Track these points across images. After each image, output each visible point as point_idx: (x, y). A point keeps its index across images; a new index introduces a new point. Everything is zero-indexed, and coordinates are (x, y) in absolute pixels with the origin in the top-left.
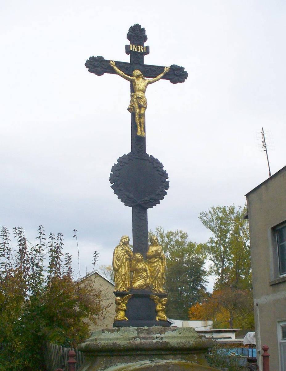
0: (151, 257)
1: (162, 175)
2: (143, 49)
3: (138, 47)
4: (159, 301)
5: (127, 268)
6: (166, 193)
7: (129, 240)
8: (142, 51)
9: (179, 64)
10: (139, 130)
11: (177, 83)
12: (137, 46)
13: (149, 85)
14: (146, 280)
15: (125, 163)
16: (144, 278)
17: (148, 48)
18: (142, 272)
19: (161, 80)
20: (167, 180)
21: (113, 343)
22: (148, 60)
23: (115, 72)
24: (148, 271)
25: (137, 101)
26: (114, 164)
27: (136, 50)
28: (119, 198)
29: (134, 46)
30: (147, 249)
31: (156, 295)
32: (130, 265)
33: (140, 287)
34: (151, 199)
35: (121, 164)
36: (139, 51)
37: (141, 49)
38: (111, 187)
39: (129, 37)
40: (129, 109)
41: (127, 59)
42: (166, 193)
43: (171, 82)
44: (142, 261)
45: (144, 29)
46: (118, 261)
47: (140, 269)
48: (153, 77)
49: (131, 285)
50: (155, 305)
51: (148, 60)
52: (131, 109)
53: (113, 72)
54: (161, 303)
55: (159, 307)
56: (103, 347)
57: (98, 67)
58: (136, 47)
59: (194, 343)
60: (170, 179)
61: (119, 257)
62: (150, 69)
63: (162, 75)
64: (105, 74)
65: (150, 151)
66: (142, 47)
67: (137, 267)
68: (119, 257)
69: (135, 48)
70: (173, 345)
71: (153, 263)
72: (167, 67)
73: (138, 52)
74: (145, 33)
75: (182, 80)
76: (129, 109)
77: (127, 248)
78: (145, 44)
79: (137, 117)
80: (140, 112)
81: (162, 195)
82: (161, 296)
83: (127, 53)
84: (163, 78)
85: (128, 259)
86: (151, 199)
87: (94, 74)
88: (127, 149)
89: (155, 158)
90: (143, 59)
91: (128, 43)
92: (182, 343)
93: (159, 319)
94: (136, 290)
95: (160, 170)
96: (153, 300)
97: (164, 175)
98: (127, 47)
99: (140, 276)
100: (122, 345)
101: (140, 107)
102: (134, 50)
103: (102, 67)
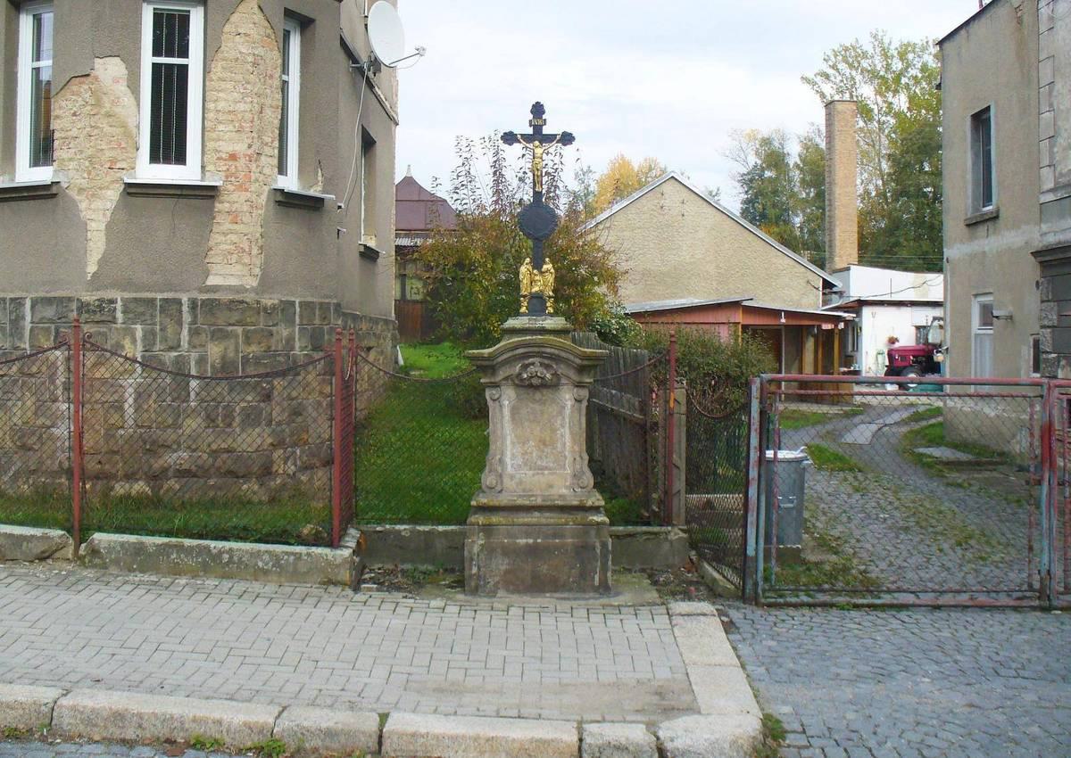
17: (545, 120)
22: (546, 130)
30: (542, 267)
41: (530, 131)
51: (546, 130)
55: (548, 304)
78: (544, 117)
82: (550, 297)
90: (541, 130)
96: (545, 300)
98: (530, 121)
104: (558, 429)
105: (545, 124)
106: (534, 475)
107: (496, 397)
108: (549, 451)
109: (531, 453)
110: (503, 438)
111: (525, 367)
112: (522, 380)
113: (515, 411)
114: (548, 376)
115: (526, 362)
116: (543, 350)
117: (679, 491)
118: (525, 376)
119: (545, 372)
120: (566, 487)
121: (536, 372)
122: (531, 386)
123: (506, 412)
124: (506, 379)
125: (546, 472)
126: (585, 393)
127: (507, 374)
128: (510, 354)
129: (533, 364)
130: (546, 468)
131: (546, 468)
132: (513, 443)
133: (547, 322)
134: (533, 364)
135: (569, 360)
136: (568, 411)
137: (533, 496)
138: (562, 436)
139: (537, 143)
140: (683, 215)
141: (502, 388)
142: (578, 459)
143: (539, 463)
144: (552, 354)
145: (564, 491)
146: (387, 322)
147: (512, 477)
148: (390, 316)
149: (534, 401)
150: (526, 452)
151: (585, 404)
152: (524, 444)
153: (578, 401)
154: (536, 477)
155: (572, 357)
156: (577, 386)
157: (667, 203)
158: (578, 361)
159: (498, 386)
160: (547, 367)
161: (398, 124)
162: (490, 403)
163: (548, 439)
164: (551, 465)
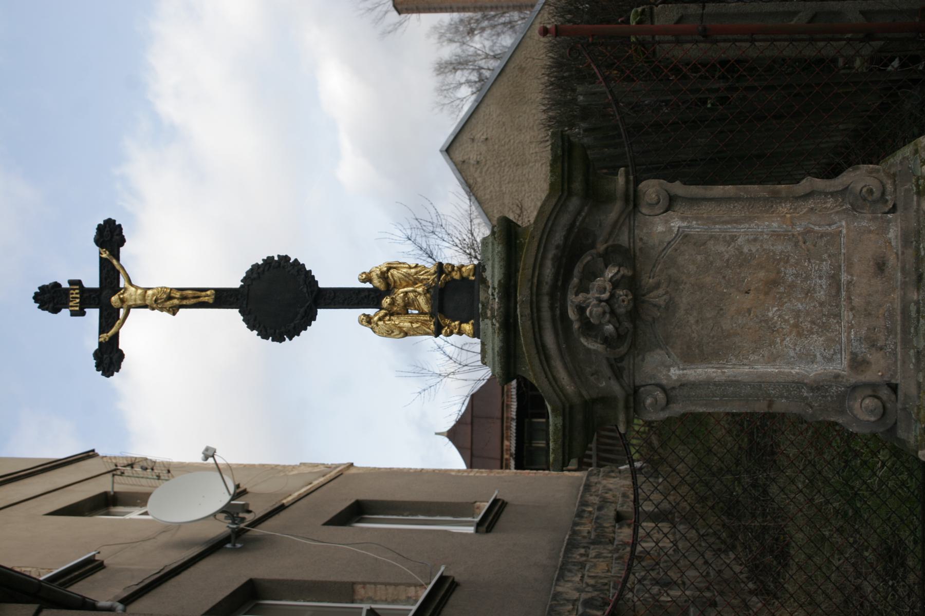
0: (388, 285)
1: (270, 266)
2: (74, 289)
3: (73, 298)
4: (447, 275)
5: (402, 318)
6: (296, 260)
7: (364, 315)
8: (77, 291)
9: (93, 232)
10: (206, 299)
11: (124, 236)
12: (71, 299)
13: (133, 282)
14: (420, 294)
15: (255, 320)
16: (416, 297)
17: (71, 282)
18: (408, 299)
19: (121, 262)
20: (276, 258)
21: (498, 355)
22: (92, 281)
23: (116, 336)
24: (406, 289)
25: (162, 302)
26: (258, 335)
27: (78, 300)
28: (306, 329)
29: (71, 304)
31: (439, 279)
32: (398, 314)
33: (427, 302)
34: (305, 283)
35: (257, 326)
36: (78, 296)
37: (74, 292)
38: (291, 339)
39: (55, 310)
40: (174, 314)
41: (93, 315)
42: (296, 260)
43: (122, 245)
44: (392, 298)
45: (39, 288)
46: (393, 332)
47: (404, 301)
48: (118, 272)
49: (425, 314)
50: (453, 280)
51: (92, 281)
52: (174, 310)
53: (115, 338)
54: (450, 272)
56: (502, 368)
57: (111, 359)
58: (72, 301)
59: (500, 246)
60: (275, 254)
61: (388, 331)
62: (106, 279)
63: (115, 262)
64: (120, 347)
65: (236, 283)
66: (72, 292)
67: (402, 304)
68: (388, 331)
69: (75, 302)
70: (502, 276)
71: (395, 282)
72: (100, 253)
73: (80, 298)
74: (47, 286)
75: (118, 229)
76: (174, 314)
77: (376, 319)
78: (65, 285)
79: (184, 302)
80: (178, 299)
81: (298, 267)
83: (81, 313)
84: (118, 259)
85: (390, 318)
86: (305, 283)
87: (122, 363)
88: (234, 315)
89: (244, 275)
91: (65, 312)
92: (500, 262)
93: (473, 276)
94: (432, 307)
95: (261, 269)
96: (447, 283)
97: (269, 261)
98: (74, 314)
99: (413, 302)
100: (501, 344)
101: (170, 298)
102: (77, 303)
103: (111, 353)
104: (740, 250)
105: (79, 283)
106: (852, 309)
107: (660, 395)
108: (790, 271)
109: (797, 314)
110: (759, 386)
111: (589, 328)
112: (620, 337)
113: (689, 357)
114: (610, 273)
115: (576, 326)
116: (546, 288)
117: (862, 12)
118: (610, 328)
119: (599, 281)
120: (884, 230)
121: (600, 301)
122: (634, 314)
123: (699, 372)
124: (618, 373)
125: (844, 277)
126: (651, 188)
127: (607, 372)
128: (558, 364)
129: (581, 309)
130: (835, 280)
131: (835, 280)
132: (772, 359)
133: (489, 279)
134: (581, 309)
135: (572, 225)
136: (696, 228)
137: (905, 311)
138: (755, 240)
139: (114, 299)
140: (487, 139)
141: (638, 382)
142: (811, 203)
143: (821, 295)
144: (557, 260)
145: (893, 233)
146: (588, 487)
147: (857, 363)
148: (582, 478)
149: (670, 306)
150: (796, 326)
151: (678, 188)
152: (773, 330)
153: (672, 202)
154: (857, 301)
155: (565, 220)
156: (636, 206)
157: (473, 157)
158: (574, 203)
159: (636, 390)
160: (591, 275)
161: (352, 464)
162: (677, 409)
163: (762, 274)
164: (825, 266)
